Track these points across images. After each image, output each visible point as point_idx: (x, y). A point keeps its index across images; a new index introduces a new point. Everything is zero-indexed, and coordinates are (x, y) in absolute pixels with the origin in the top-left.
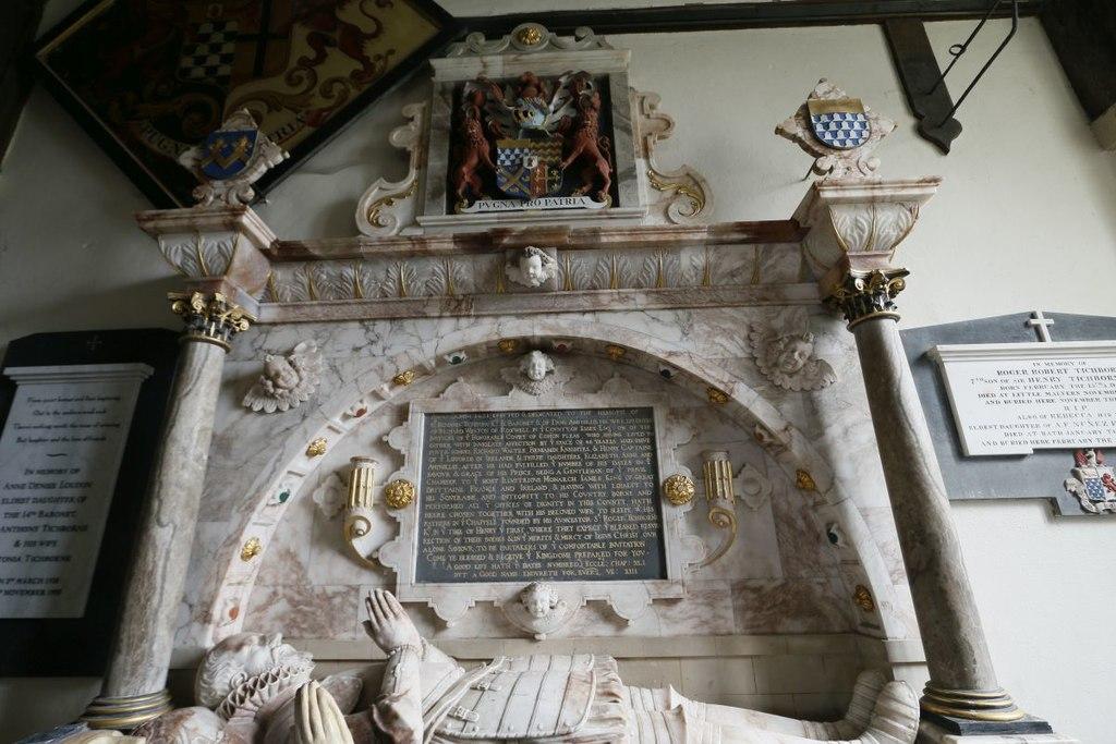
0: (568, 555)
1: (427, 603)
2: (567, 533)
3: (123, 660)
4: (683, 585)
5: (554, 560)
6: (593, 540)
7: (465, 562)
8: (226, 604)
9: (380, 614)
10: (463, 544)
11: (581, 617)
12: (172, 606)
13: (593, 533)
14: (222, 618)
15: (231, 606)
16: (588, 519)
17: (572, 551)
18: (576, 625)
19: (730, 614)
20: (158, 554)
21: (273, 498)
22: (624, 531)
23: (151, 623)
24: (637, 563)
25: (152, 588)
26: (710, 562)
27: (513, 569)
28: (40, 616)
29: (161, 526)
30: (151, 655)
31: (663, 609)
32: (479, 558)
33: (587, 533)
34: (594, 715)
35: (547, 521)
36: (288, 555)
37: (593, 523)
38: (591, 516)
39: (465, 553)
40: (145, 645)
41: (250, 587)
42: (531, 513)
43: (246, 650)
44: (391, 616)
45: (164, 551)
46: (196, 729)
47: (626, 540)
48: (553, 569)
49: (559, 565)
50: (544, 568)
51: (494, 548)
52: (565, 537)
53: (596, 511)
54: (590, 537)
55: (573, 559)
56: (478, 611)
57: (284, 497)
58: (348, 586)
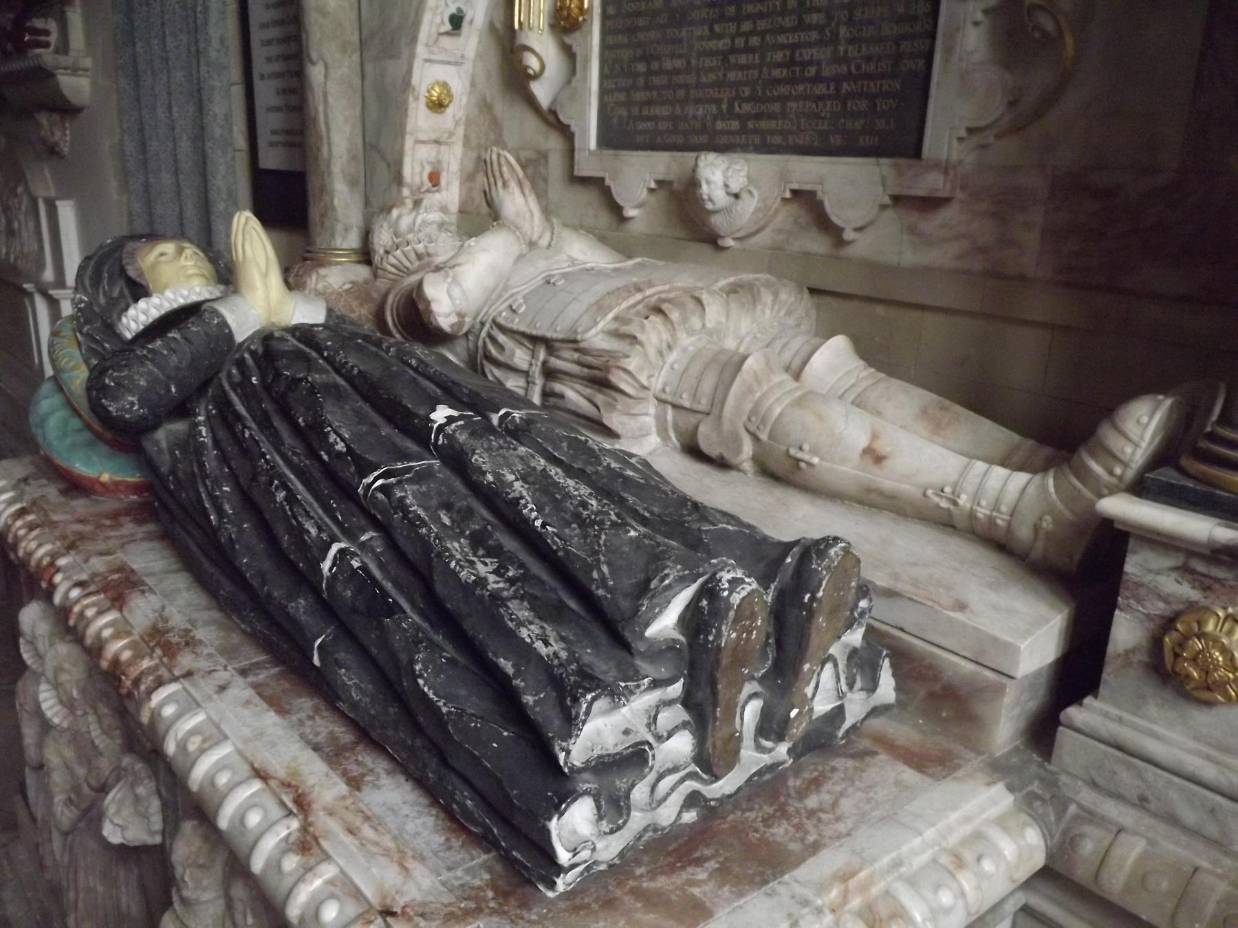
0: (776, 107)
1: (603, 179)
2: (779, 65)
3: (314, 212)
4: (946, 172)
5: (758, 116)
6: (817, 79)
7: (649, 119)
8: (423, 167)
9: (492, 180)
10: (647, 87)
11: (785, 217)
12: (345, 158)
13: (819, 63)
14: (422, 184)
15: (428, 169)
16: (814, 35)
17: (784, 99)
18: (779, 231)
19: (1032, 239)
20: (317, 98)
21: (443, 22)
22: (869, 59)
23: (326, 175)
24: (880, 124)
25: (321, 137)
26: (1016, 128)
27: (704, 130)
28: (282, 167)
29: (313, 64)
30: (333, 209)
31: (913, 217)
32: (663, 111)
33: (810, 63)
34: (614, 326)
35: (755, 41)
36: (485, 106)
37: (820, 43)
38: (820, 28)
39: (649, 103)
40: (326, 198)
41: (458, 150)
42: (732, 27)
43: (395, 213)
44: (500, 183)
45: (321, 94)
46: (325, 276)
47: (869, 77)
48: (756, 131)
49: (764, 125)
50: (743, 130)
51: (681, 93)
52: (777, 73)
53: (829, 17)
54: (813, 70)
55: (784, 114)
56: (662, 194)
57: (457, 21)
58: (538, 152)
